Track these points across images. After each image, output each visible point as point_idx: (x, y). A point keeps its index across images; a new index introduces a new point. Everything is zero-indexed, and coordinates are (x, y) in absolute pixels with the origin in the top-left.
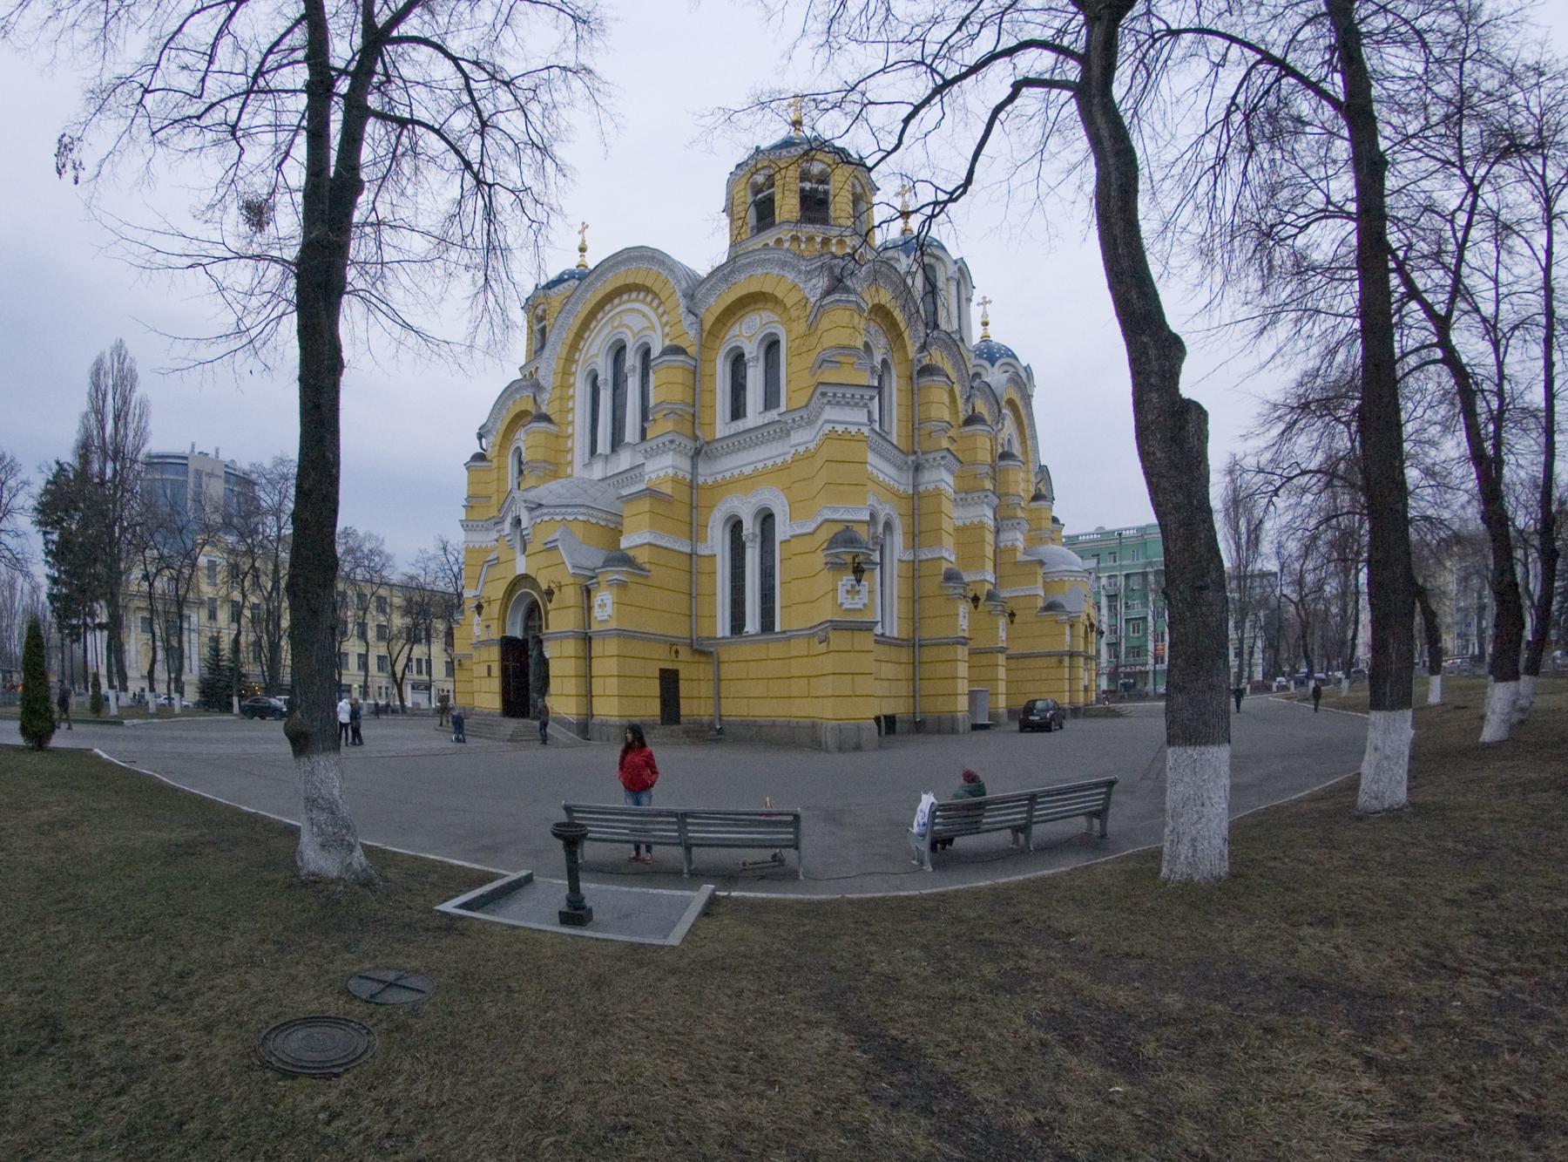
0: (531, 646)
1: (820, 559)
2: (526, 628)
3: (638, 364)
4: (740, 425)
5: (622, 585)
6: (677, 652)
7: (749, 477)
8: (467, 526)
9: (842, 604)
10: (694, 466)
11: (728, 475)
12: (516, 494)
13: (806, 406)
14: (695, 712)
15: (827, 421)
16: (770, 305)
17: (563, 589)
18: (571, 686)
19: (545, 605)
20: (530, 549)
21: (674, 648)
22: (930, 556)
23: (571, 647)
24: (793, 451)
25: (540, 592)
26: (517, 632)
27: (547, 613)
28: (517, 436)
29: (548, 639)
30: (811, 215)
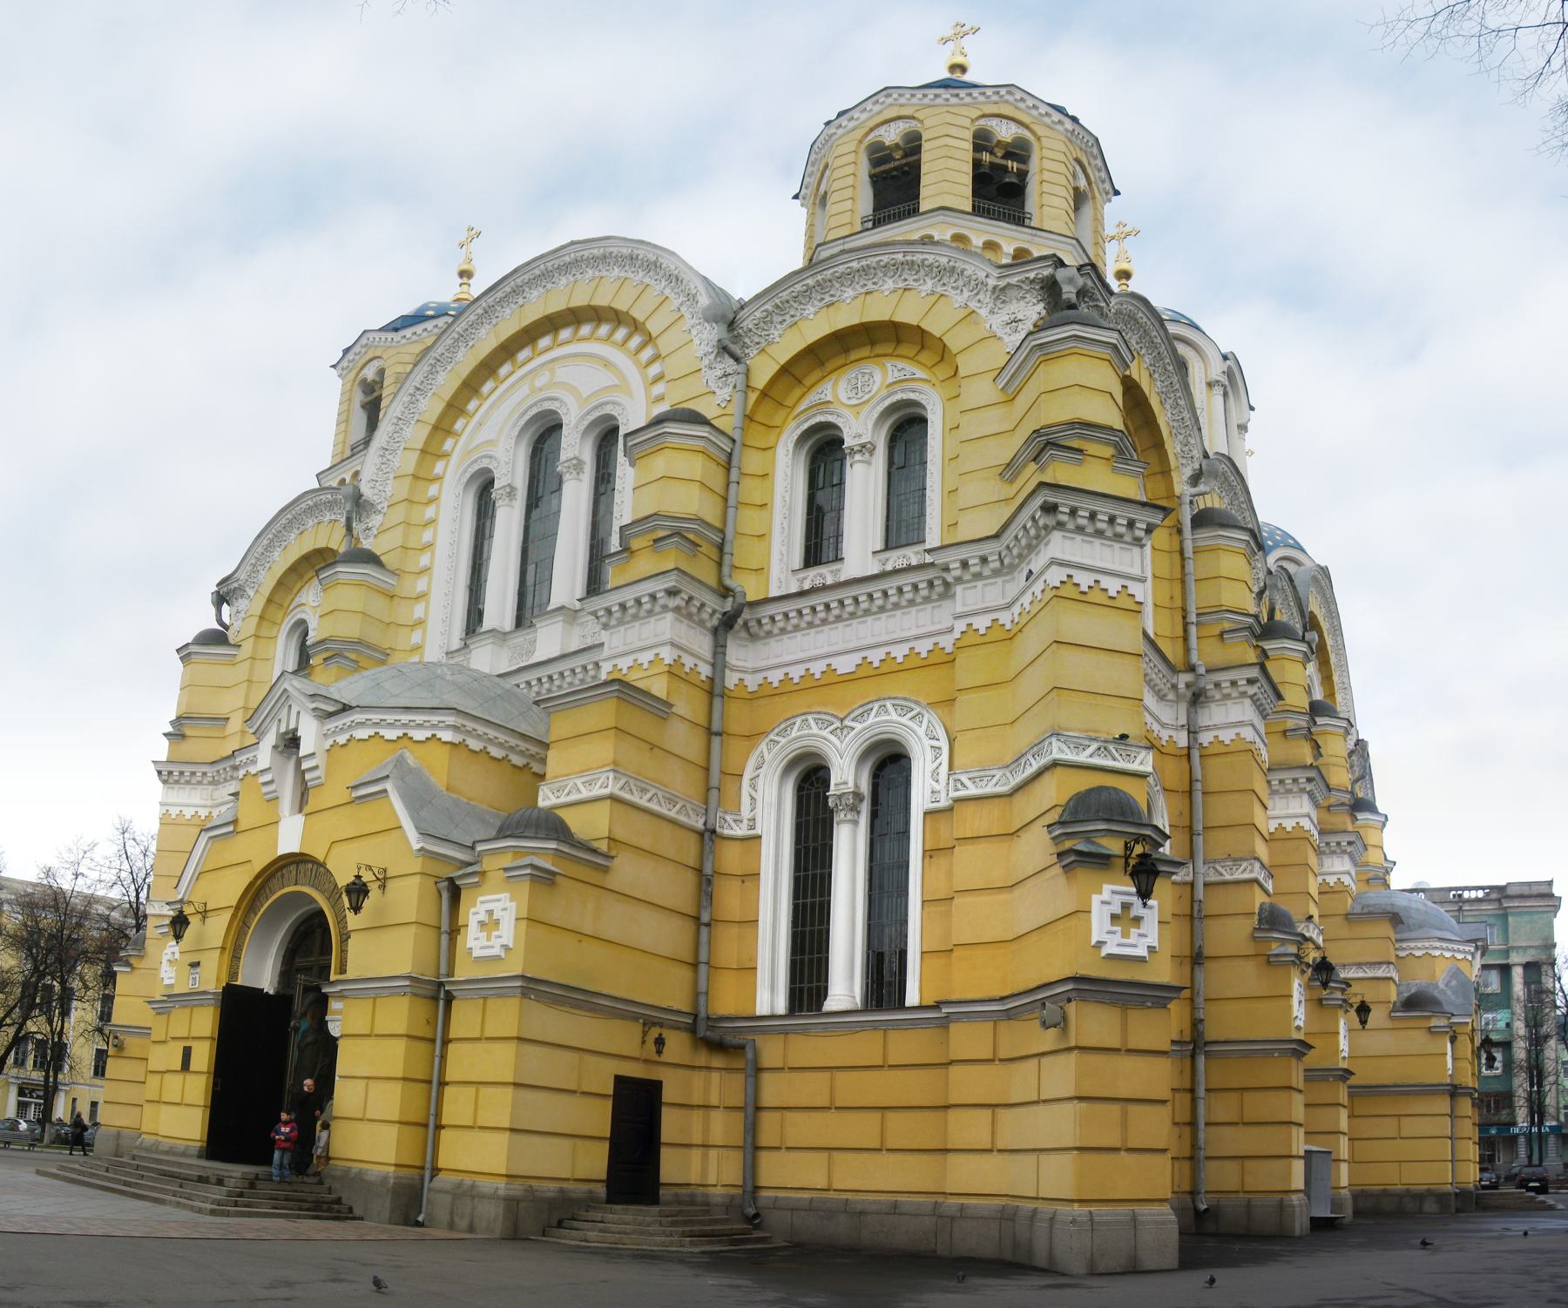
0: (298, 1006)
1: (1037, 848)
2: (287, 973)
3: (588, 455)
4: (824, 574)
5: (544, 879)
6: (660, 1042)
7: (850, 678)
8: (168, 774)
9: (1100, 944)
10: (719, 649)
11: (796, 673)
12: (294, 685)
13: (997, 536)
14: (694, 1178)
15: (1055, 562)
16: (908, 350)
17: (390, 885)
18: (389, 1101)
19: (342, 921)
20: (313, 803)
21: (654, 1033)
22: (1228, 877)
23: (398, 1014)
24: (960, 626)
25: (333, 893)
26: (263, 975)
27: (345, 937)
28: (301, 598)
29: (341, 996)
30: (986, 204)
